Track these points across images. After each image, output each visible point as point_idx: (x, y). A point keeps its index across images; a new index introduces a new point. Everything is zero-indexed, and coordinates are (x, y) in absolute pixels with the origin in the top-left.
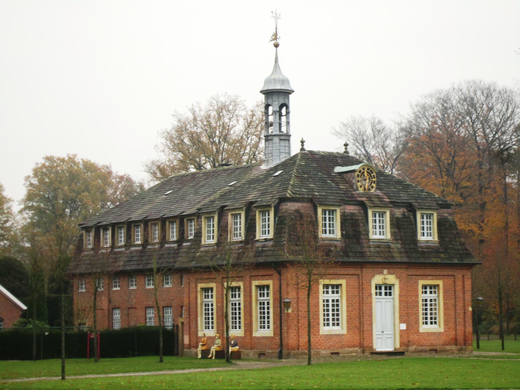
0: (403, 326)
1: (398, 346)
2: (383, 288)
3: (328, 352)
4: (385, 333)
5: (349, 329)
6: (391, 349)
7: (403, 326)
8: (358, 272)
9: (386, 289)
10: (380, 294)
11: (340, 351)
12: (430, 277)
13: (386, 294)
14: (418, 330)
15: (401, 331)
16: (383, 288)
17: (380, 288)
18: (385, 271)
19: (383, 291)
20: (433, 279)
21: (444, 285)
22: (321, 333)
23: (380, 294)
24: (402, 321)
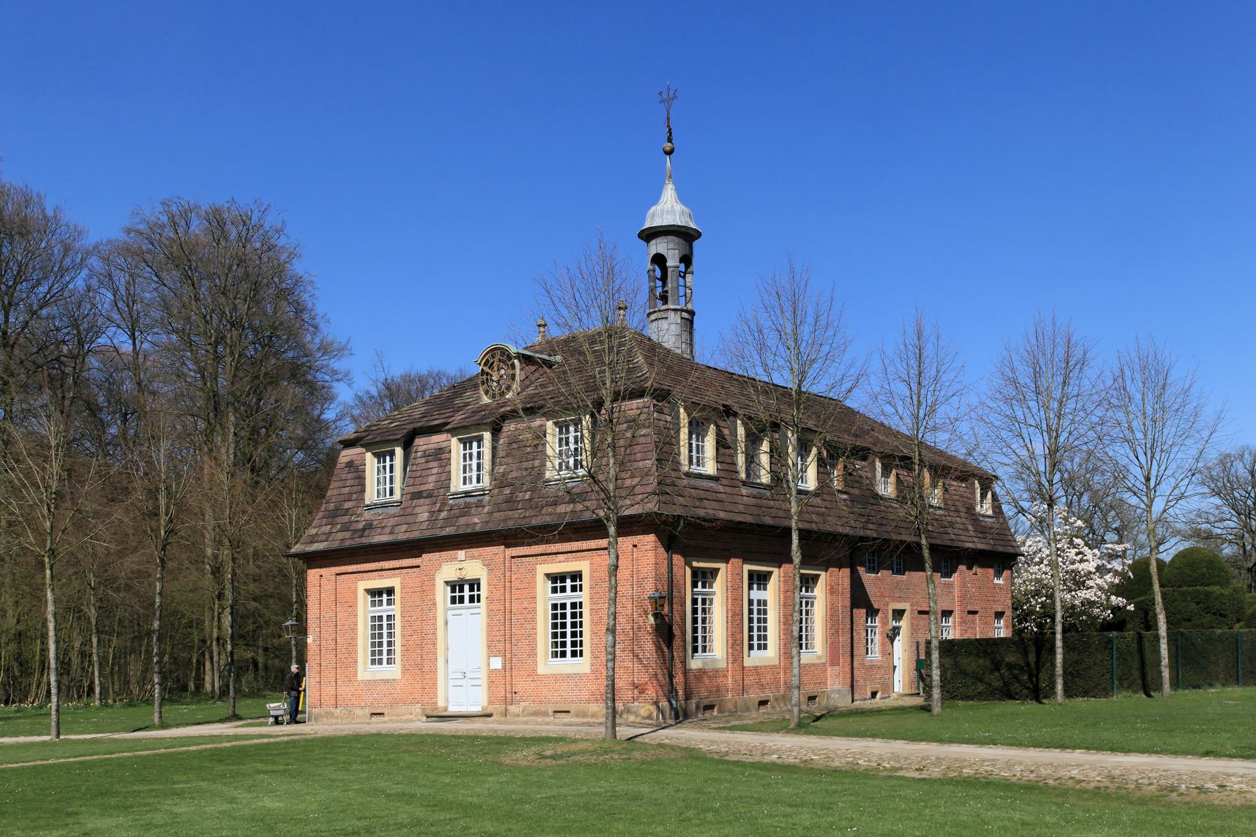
1: (485, 704)
2: (466, 587)
3: (368, 711)
4: (468, 675)
5: (405, 670)
6: (477, 709)
10: (461, 600)
11: (385, 711)
12: (561, 557)
14: (535, 670)
15: (492, 671)
16: (466, 587)
17: (461, 590)
18: (461, 554)
19: (467, 593)
20: (567, 560)
22: (359, 678)
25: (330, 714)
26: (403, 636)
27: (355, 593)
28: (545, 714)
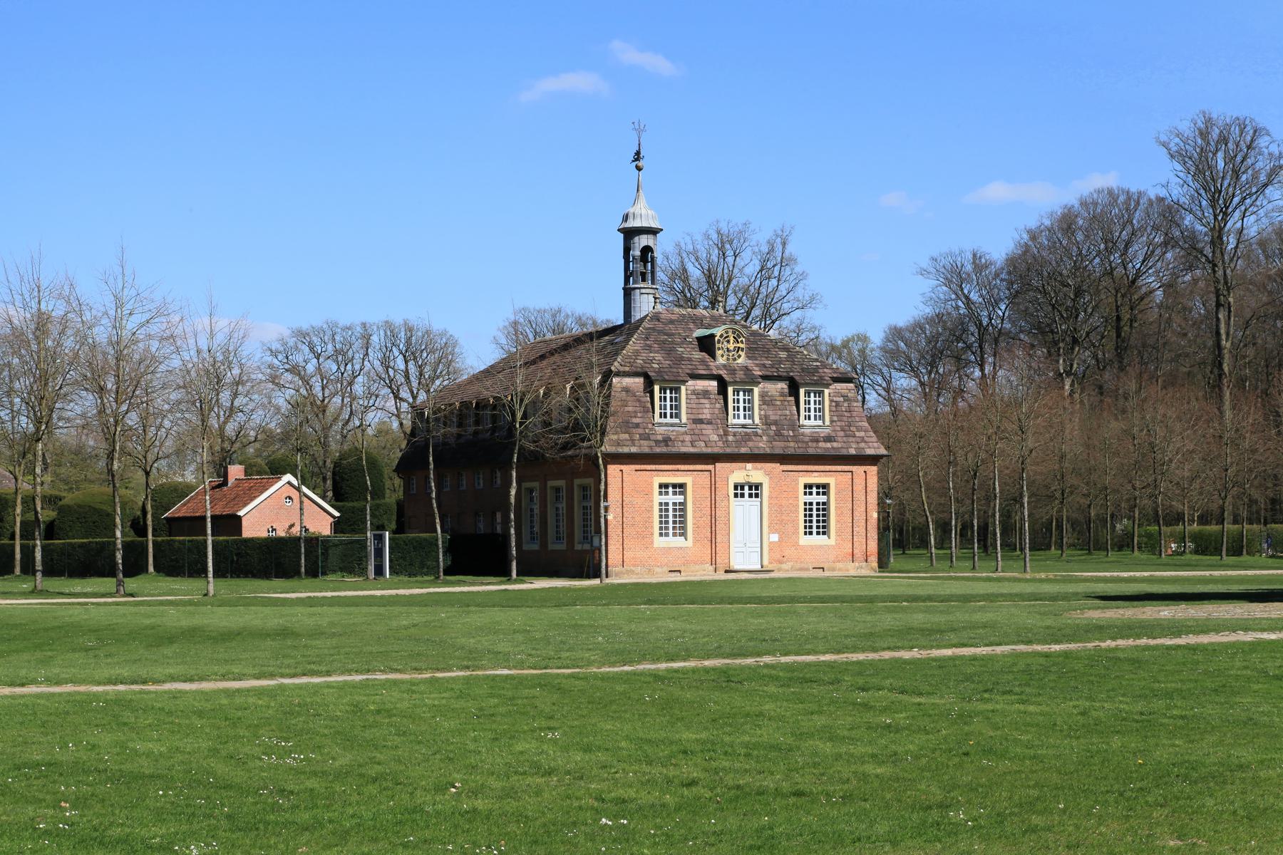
0: (775, 538)
2: (746, 488)
3: (666, 569)
5: (696, 540)
7: (775, 538)
8: (710, 467)
9: (750, 488)
10: (742, 495)
13: (750, 496)
16: (746, 488)
17: (742, 488)
19: (746, 491)
21: (837, 484)
22: (656, 545)
23: (742, 495)
24: (771, 531)
25: (632, 572)
26: (694, 517)
27: (651, 484)
28: (807, 569)
